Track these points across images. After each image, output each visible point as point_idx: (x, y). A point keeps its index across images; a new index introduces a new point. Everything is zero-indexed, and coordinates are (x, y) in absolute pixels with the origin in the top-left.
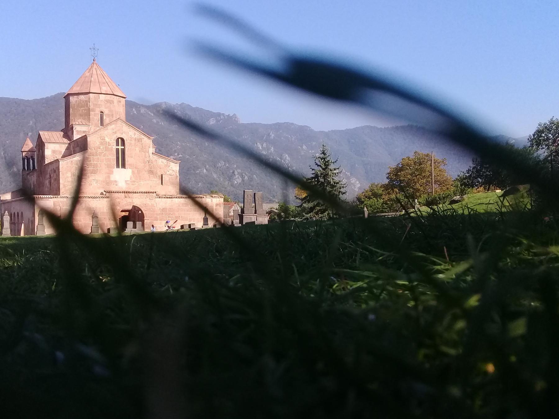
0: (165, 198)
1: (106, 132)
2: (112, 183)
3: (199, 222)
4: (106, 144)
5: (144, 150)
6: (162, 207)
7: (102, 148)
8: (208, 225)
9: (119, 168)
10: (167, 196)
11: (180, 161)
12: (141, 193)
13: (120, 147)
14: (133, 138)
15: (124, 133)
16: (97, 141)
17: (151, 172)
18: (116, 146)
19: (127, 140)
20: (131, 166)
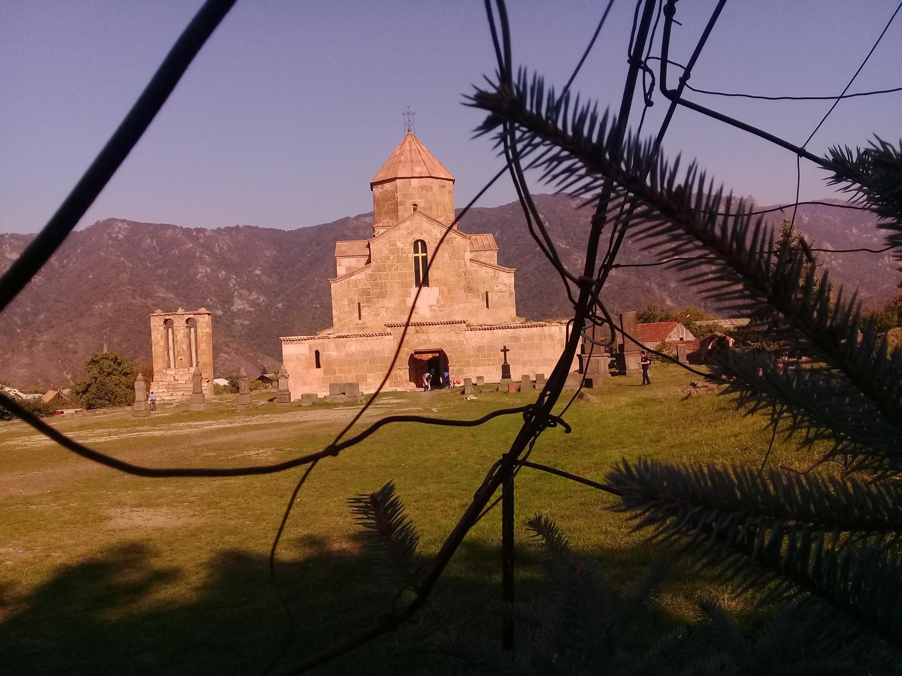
0: (480, 330)
1: (397, 234)
3: (539, 366)
7: (392, 258)
11: (516, 269)
12: (442, 324)
13: (420, 255)
17: (469, 289)
19: (429, 242)
20: (438, 282)
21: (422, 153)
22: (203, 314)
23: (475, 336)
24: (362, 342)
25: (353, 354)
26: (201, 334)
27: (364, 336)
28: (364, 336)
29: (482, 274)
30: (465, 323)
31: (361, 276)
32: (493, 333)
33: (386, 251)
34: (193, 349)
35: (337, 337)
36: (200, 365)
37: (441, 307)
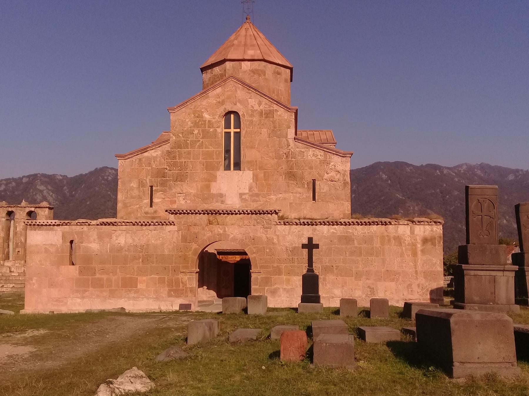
0: (297, 224)
1: (204, 103)
2: (215, 199)
3: (380, 280)
4: (205, 124)
5: (279, 133)
6: (292, 244)
7: (196, 132)
8: (316, 299)
12: (244, 214)
13: (232, 130)
16: (187, 120)
17: (291, 175)
19: (244, 115)
20: (252, 164)
23: (289, 233)
28: (138, 224)
30: (277, 213)
31: (156, 153)
33: (189, 123)
35: (102, 225)
37: (255, 196)
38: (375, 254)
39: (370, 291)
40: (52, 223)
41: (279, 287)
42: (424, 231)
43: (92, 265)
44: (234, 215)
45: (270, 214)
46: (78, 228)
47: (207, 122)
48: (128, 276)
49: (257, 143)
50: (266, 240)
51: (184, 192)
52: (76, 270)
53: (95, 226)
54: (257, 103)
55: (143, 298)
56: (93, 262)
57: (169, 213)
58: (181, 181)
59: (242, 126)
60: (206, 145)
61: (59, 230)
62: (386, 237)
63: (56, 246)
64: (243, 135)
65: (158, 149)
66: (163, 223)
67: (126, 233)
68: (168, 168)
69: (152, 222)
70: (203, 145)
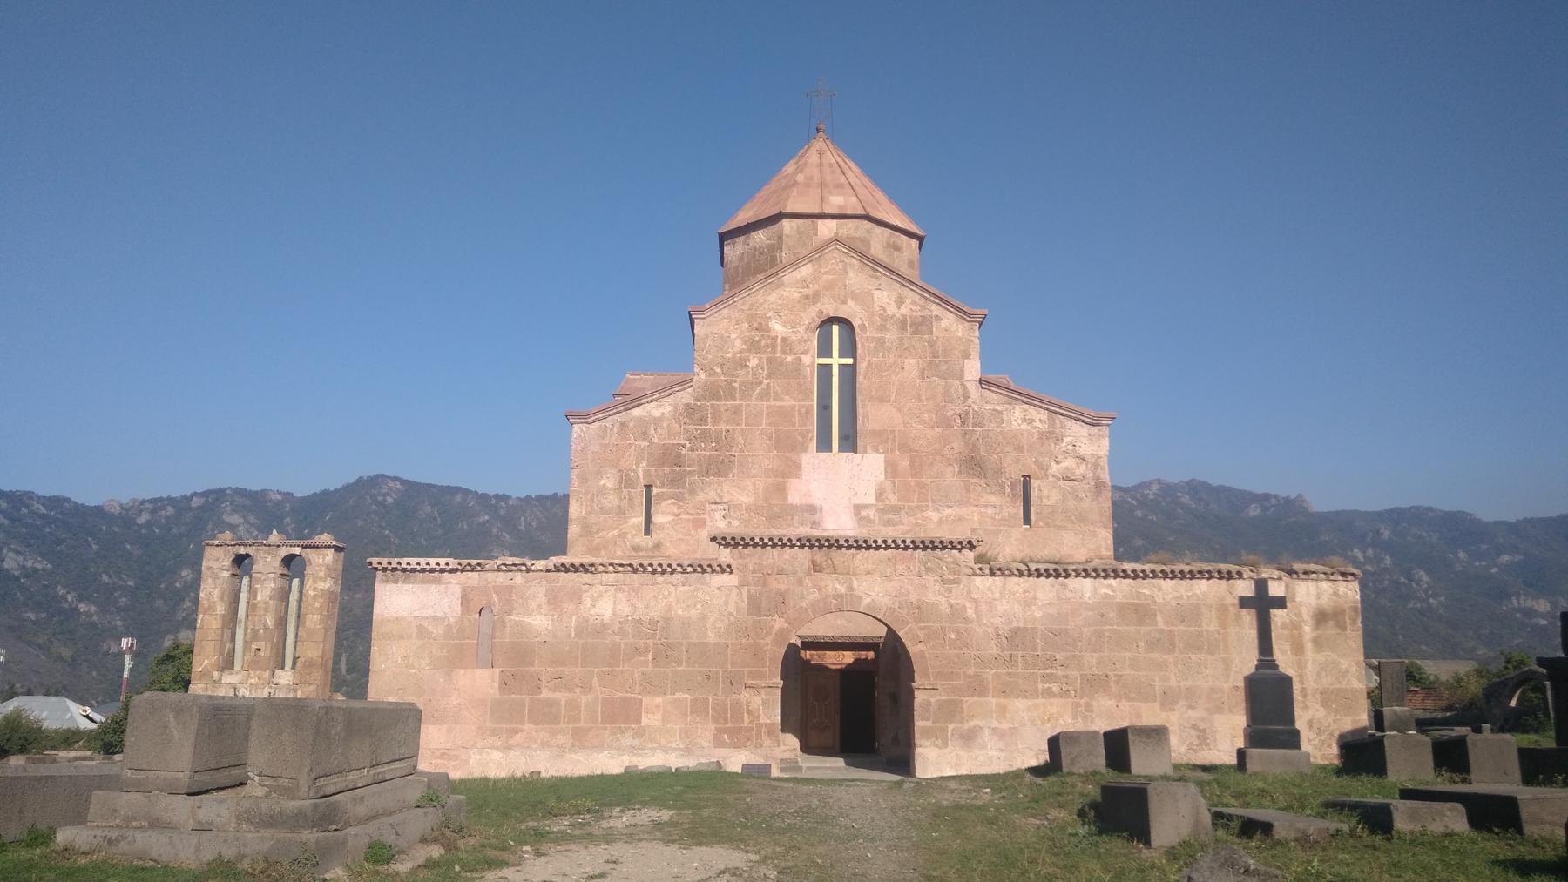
0: (1021, 574)
3: (1219, 710)
4: (774, 346)
5: (944, 368)
6: (1010, 622)
7: (753, 362)
9: (830, 449)
10: (1033, 567)
12: (897, 547)
13: (836, 361)
14: (894, 316)
15: (854, 296)
16: (733, 336)
17: (973, 465)
18: (820, 356)
19: (863, 327)
20: (883, 439)
21: (849, 173)
22: (322, 547)
23: (1002, 594)
24: (636, 591)
25: (604, 626)
26: (311, 593)
27: (645, 570)
28: (645, 570)
29: (1014, 423)
32: (1065, 587)
34: (291, 628)
35: (558, 570)
36: (299, 664)
37: (889, 511)
38: (1206, 647)
39: (1198, 737)
40: (438, 564)
41: (980, 723)
42: (1318, 594)
43: (533, 669)
44: (872, 550)
45: (958, 549)
46: (501, 578)
47: (779, 340)
48: (619, 695)
49: (894, 389)
50: (947, 611)
51: (725, 500)
52: (493, 681)
53: (541, 573)
54: (893, 300)
55: (653, 749)
56: (534, 661)
57: (720, 544)
58: (718, 474)
59: (859, 351)
60: (777, 392)
61: (454, 582)
62: (1231, 608)
63: (447, 620)
64: (862, 372)
65: (665, 399)
66: (705, 567)
67: (616, 590)
68: (688, 445)
69: (679, 565)
70: (770, 393)
